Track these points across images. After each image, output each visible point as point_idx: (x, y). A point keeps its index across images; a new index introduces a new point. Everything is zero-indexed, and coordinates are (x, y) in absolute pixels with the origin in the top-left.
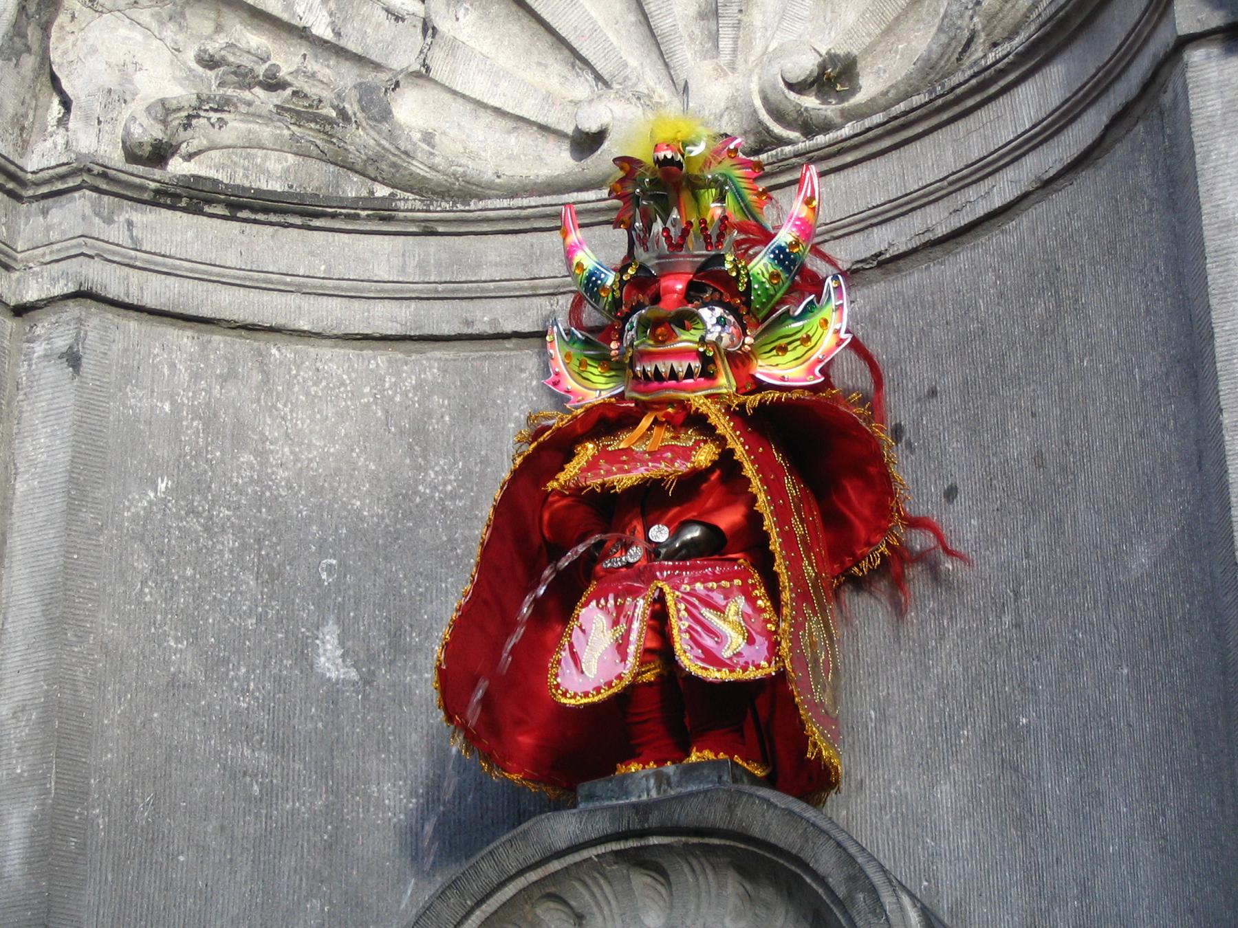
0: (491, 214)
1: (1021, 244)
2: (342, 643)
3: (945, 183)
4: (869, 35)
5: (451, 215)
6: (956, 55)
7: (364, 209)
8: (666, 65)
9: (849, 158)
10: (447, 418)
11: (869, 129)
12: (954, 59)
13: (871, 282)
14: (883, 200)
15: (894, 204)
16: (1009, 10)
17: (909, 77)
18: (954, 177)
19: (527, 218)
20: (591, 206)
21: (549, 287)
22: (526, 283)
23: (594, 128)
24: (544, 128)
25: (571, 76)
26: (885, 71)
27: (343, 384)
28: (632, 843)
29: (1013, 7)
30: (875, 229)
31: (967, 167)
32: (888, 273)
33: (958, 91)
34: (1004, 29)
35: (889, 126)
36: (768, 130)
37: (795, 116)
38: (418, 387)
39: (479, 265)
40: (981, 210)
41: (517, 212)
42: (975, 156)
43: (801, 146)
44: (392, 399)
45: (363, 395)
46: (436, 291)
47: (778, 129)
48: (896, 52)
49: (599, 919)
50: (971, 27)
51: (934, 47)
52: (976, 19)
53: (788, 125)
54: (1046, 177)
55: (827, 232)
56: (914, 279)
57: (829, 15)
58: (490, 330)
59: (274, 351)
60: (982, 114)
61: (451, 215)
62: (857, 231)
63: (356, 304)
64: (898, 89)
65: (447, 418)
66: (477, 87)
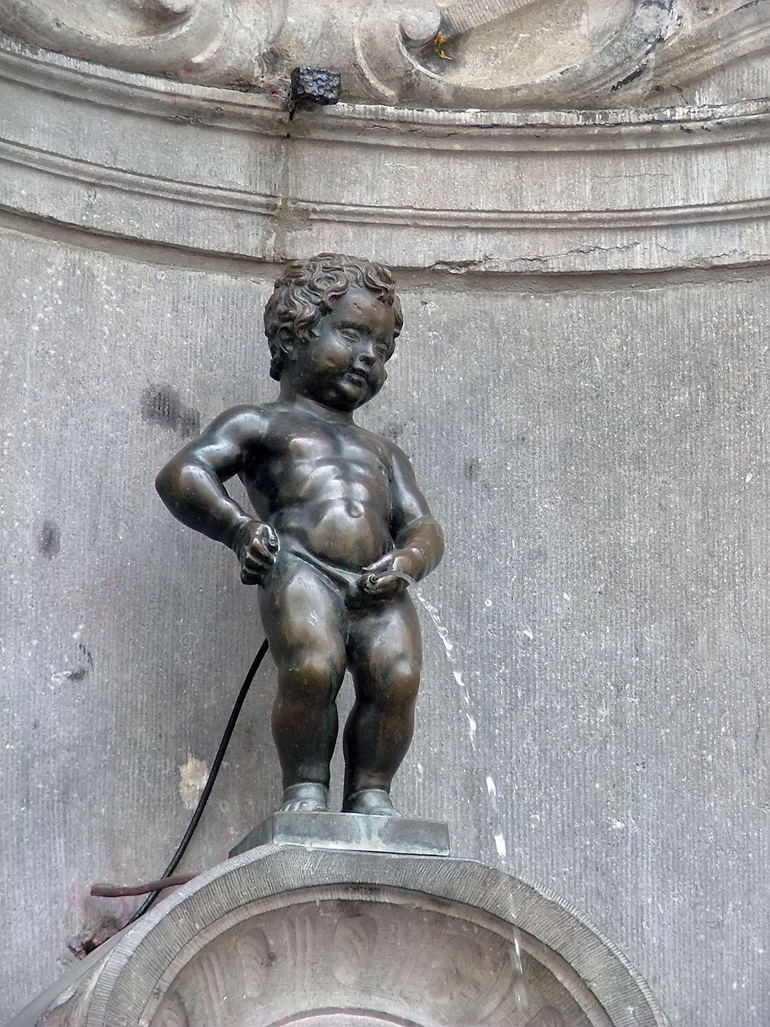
0: (55, 72)
1: (663, 319)
3: (575, 218)
4: (493, 10)
5: (16, 60)
6: (615, 83)
12: (610, 85)
13: (451, 289)
14: (490, 207)
15: (502, 216)
16: (692, 60)
17: (550, 83)
18: (589, 216)
19: (86, 88)
20: (156, 96)
22: (70, 164)
26: (496, 56)
28: (358, 896)
29: (697, 58)
30: (469, 234)
31: (607, 211)
33: (624, 130)
34: (677, 77)
35: (520, 132)
37: (402, 74)
40: (614, 262)
41: (80, 78)
42: (624, 203)
48: (515, 39)
49: (292, 962)
50: (644, 61)
51: (593, 65)
52: (652, 56)
53: (388, 82)
54: (716, 262)
55: (413, 217)
60: (644, 164)
61: (16, 60)
62: (446, 228)
64: (531, 90)
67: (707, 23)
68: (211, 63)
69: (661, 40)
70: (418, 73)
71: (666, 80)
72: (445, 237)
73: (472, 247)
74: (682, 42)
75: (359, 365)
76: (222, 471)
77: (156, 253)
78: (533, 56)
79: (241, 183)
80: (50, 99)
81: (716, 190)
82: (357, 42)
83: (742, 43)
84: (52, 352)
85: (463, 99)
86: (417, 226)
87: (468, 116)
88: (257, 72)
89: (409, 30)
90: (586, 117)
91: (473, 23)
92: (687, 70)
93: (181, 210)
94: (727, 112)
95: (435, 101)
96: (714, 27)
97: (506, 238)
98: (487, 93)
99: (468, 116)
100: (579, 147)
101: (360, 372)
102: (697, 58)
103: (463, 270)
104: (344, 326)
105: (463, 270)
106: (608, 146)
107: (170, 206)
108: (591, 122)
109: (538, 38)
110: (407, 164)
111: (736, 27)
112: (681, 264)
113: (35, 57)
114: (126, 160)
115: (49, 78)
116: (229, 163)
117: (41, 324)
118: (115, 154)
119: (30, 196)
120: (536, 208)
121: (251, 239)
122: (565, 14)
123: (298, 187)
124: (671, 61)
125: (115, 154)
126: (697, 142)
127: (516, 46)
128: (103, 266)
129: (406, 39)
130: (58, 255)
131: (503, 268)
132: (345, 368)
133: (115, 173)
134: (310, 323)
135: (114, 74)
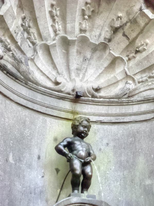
0: (41, 90)
2: (13, 157)
3: (116, 114)
4: (105, 85)
6: (122, 95)
7: (24, 81)
8: (70, 75)
9: (100, 104)
10: (28, 122)
11: (105, 101)
12: (122, 96)
13: (98, 124)
14: (104, 113)
17: (113, 95)
19: (46, 93)
20: (56, 95)
21: (46, 106)
22: (43, 104)
23: (60, 82)
24: (48, 77)
25: (53, 69)
27: (15, 111)
29: (134, 92)
30: (101, 117)
32: (101, 124)
33: (124, 102)
36: (86, 94)
38: (25, 115)
39: (37, 98)
40: (122, 121)
41: (45, 91)
42: (123, 112)
43: (90, 99)
44: (21, 116)
45: (17, 114)
46: (30, 100)
47: (88, 94)
52: (128, 91)
53: (90, 95)
56: (106, 127)
57: (98, 79)
58: (37, 110)
59: (7, 101)
60: (126, 106)
63: (19, 97)
65: (28, 122)
66: (39, 65)
67: (136, 87)
68: (64, 91)
69: (129, 89)
70: (94, 93)
71: (130, 95)
72: (98, 117)
73: (102, 118)
74: (132, 89)
75: (85, 132)
76: (65, 146)
77: (55, 118)
78: (111, 92)
79: (68, 108)
80: (40, 94)
81: (137, 110)
82: (86, 89)
83: (141, 90)
84: (40, 131)
85: (101, 97)
86: (93, 115)
87: (101, 100)
88: (71, 92)
89: (93, 87)
90: (118, 100)
91: (103, 87)
92: (133, 94)
93: (59, 112)
94: (140, 99)
95: (96, 97)
96: (137, 87)
97: (106, 117)
98: (104, 97)
99: (101, 100)
100: (117, 104)
101: (85, 133)
102: (134, 92)
103: (100, 122)
104: (83, 126)
105: (100, 122)
106: (121, 104)
107: (58, 111)
108: (119, 101)
109: (112, 89)
110: (92, 106)
111: (141, 87)
112: (131, 121)
113: (38, 87)
114: (52, 104)
115: (40, 91)
116: (67, 105)
117: (38, 127)
118: (50, 103)
119: (37, 108)
120: (111, 113)
121: (70, 116)
122: (116, 86)
123: (77, 109)
124: (131, 92)
125: (50, 103)
126: (134, 103)
127: (108, 90)
128: (48, 119)
129: (93, 88)
130: (41, 117)
131: (106, 121)
132: (83, 132)
133: (50, 106)
134: (78, 126)
135: (50, 91)
